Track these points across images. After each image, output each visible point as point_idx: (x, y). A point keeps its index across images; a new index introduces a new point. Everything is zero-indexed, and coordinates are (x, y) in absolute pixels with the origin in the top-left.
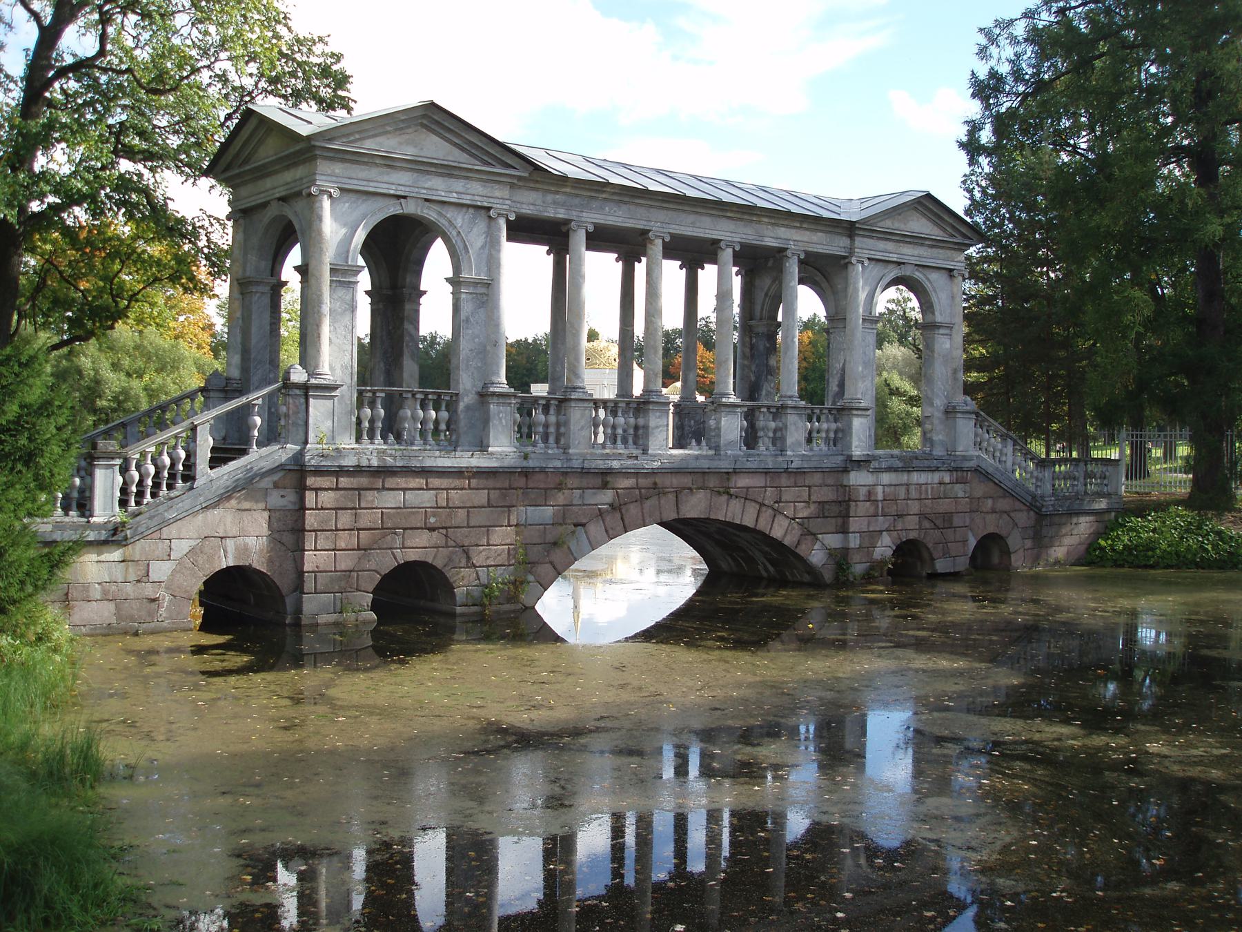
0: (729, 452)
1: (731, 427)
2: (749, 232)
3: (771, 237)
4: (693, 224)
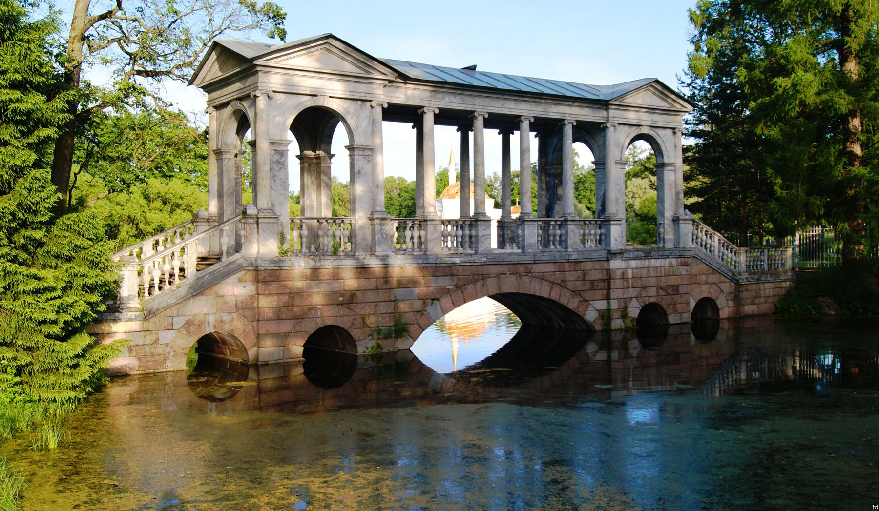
0: (530, 250)
1: (532, 234)
2: (540, 110)
3: (554, 111)
4: (502, 107)
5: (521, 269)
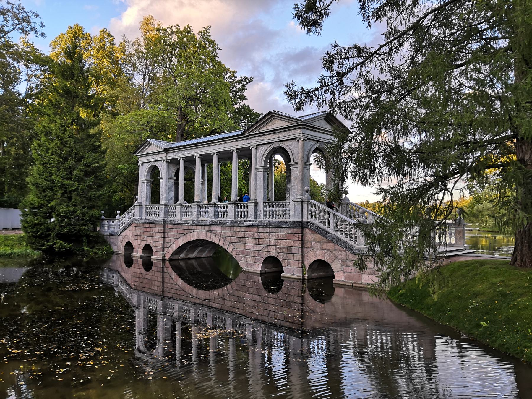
5: (207, 228)
